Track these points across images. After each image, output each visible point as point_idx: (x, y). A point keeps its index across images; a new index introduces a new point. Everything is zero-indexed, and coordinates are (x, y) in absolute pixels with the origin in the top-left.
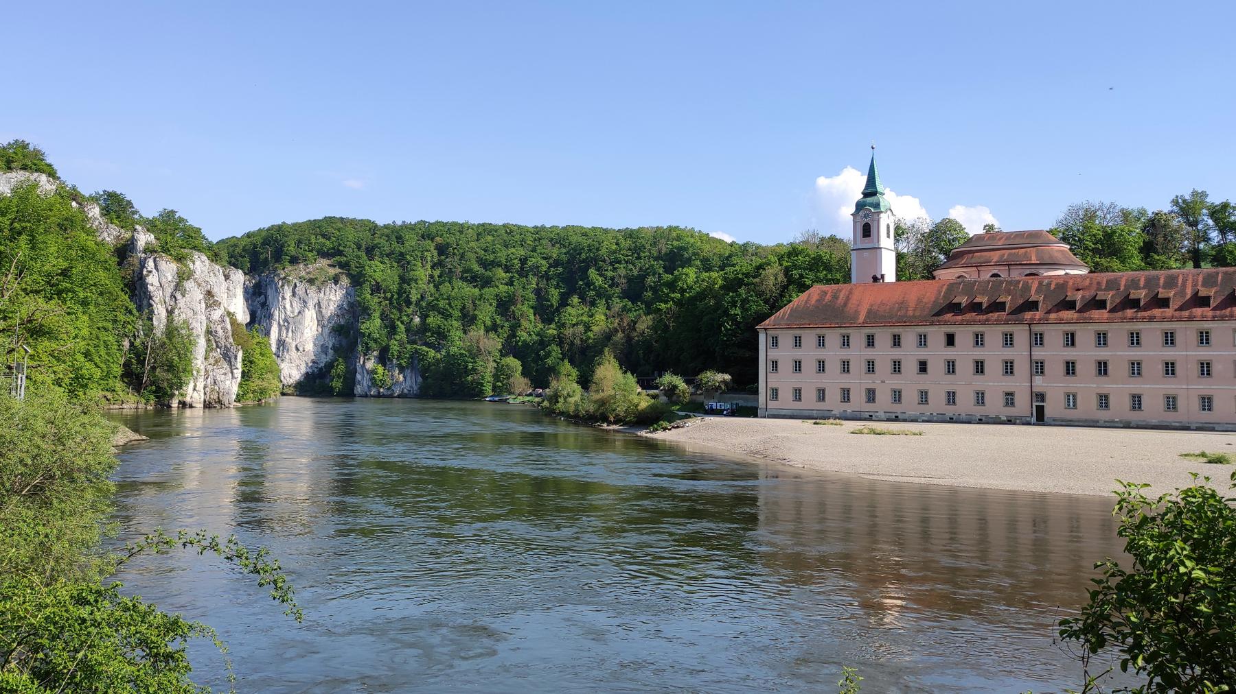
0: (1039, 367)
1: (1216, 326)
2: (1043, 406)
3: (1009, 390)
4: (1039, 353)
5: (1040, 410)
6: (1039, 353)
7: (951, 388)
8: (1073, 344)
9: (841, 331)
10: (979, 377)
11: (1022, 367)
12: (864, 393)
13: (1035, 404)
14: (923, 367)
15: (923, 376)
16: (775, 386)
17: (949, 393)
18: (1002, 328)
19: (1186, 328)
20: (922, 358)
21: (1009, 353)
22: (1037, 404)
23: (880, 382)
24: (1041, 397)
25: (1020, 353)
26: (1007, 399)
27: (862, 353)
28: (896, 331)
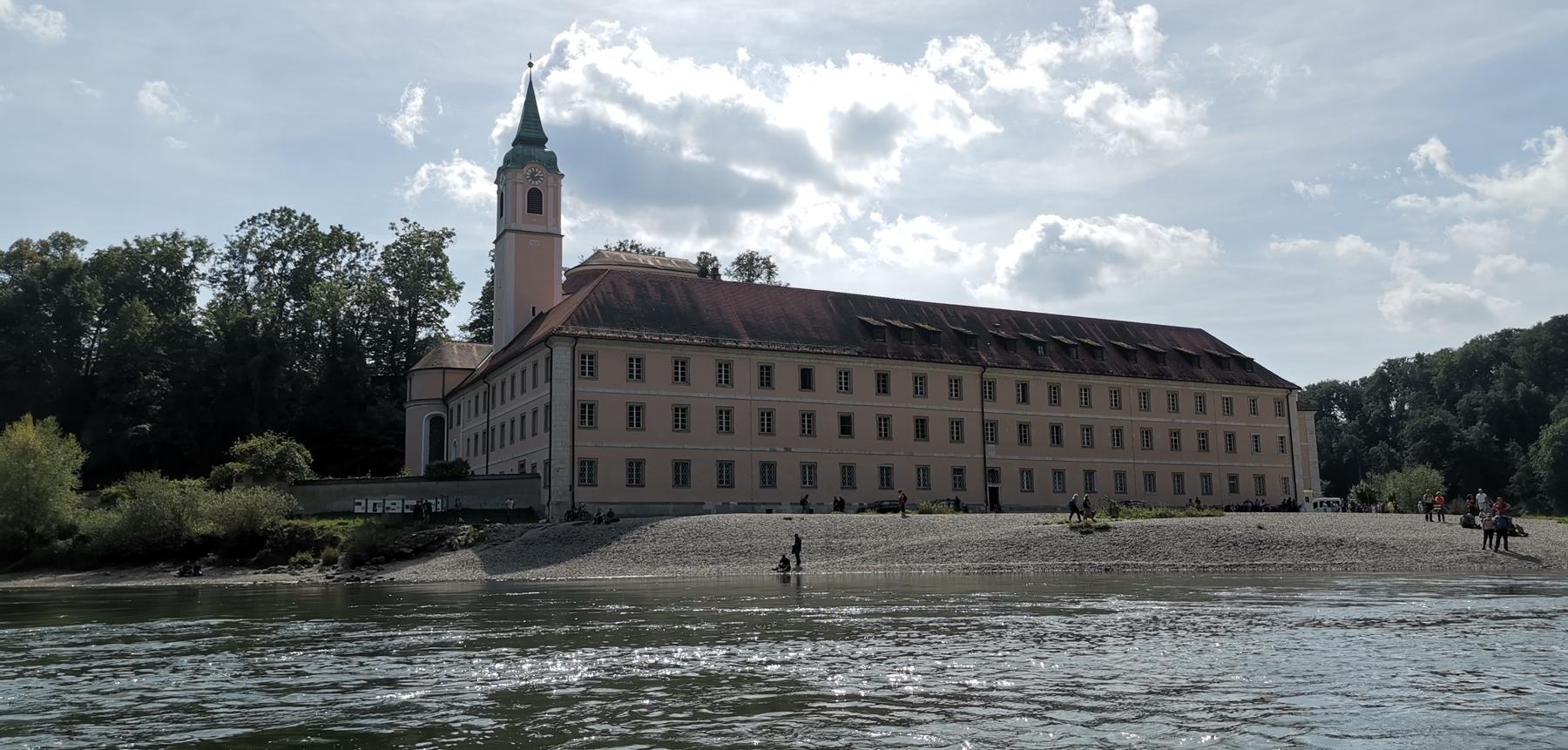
0: (990, 431)
1: (1154, 386)
2: (997, 488)
3: (958, 464)
4: (992, 410)
5: (994, 492)
6: (992, 410)
7: (885, 462)
8: (1025, 400)
9: (718, 355)
10: (922, 444)
11: (972, 430)
12: (757, 470)
13: (988, 486)
14: (846, 425)
15: (846, 441)
16: (590, 455)
17: (882, 468)
18: (949, 371)
19: (1129, 386)
20: (846, 410)
21: (956, 408)
22: (991, 486)
23: (783, 450)
24: (992, 474)
25: (969, 408)
26: (955, 478)
27: (754, 398)
28: (807, 362)
